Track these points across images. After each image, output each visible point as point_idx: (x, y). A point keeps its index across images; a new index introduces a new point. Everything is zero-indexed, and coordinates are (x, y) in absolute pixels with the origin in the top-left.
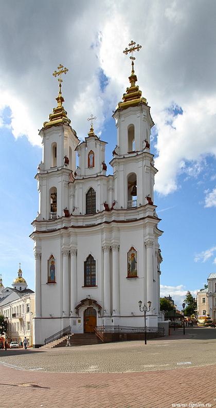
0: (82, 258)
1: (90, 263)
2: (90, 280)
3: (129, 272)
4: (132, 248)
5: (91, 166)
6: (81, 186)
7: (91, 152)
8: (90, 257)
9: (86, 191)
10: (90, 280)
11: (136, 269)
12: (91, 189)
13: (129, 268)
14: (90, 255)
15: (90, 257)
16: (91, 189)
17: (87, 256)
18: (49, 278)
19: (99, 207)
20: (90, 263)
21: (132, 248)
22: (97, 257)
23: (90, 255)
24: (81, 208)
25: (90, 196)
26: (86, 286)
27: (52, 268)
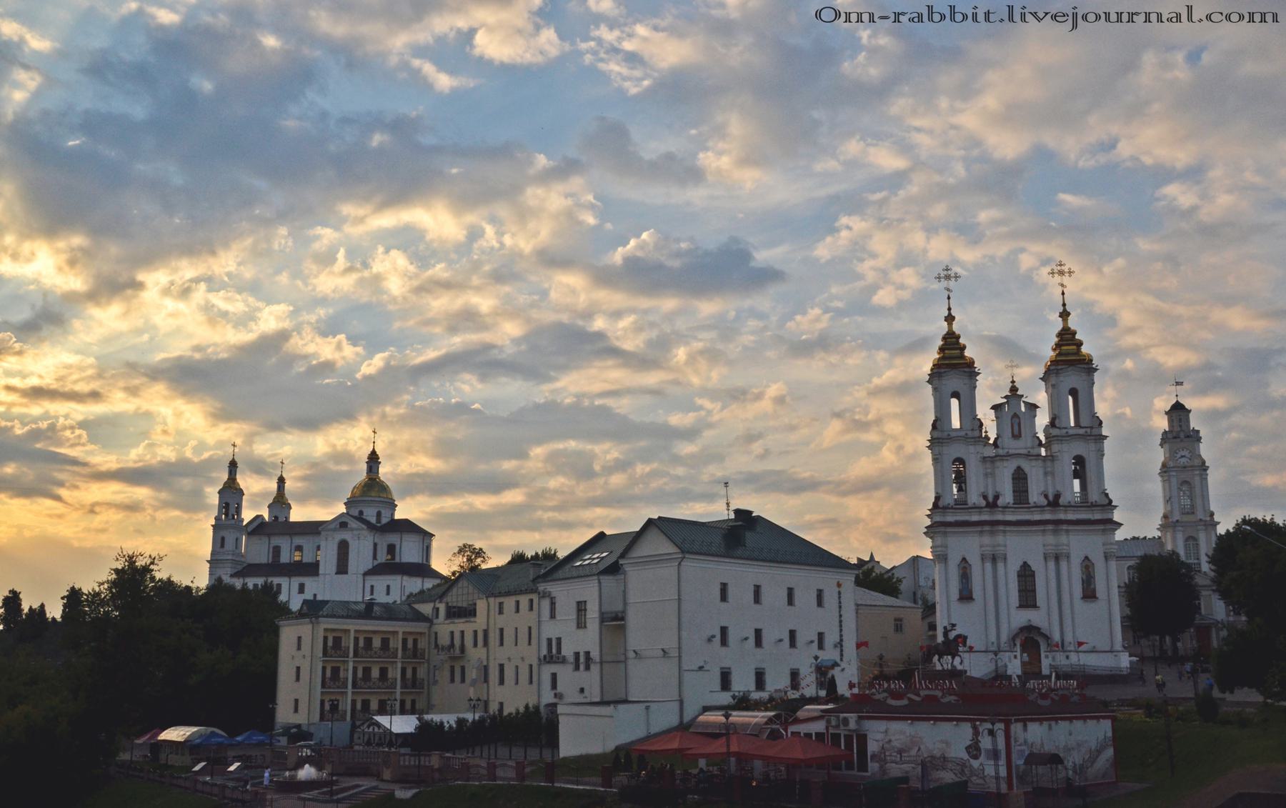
0: (1014, 566)
1: (1026, 574)
2: (1028, 598)
3: (1083, 589)
4: (1086, 558)
5: (1017, 436)
6: (1005, 464)
7: (1015, 416)
8: (1025, 566)
9: (1012, 471)
10: (1028, 598)
11: (1092, 586)
12: (1019, 468)
13: (1083, 585)
14: (1025, 563)
15: (1025, 566)
16: (1019, 468)
17: (1021, 563)
18: (961, 591)
19: (1035, 496)
20: (1026, 574)
21: (1086, 558)
22: (1037, 565)
23: (1025, 563)
24: (1007, 497)
25: (1020, 478)
26: (1021, 606)
27: (965, 576)
